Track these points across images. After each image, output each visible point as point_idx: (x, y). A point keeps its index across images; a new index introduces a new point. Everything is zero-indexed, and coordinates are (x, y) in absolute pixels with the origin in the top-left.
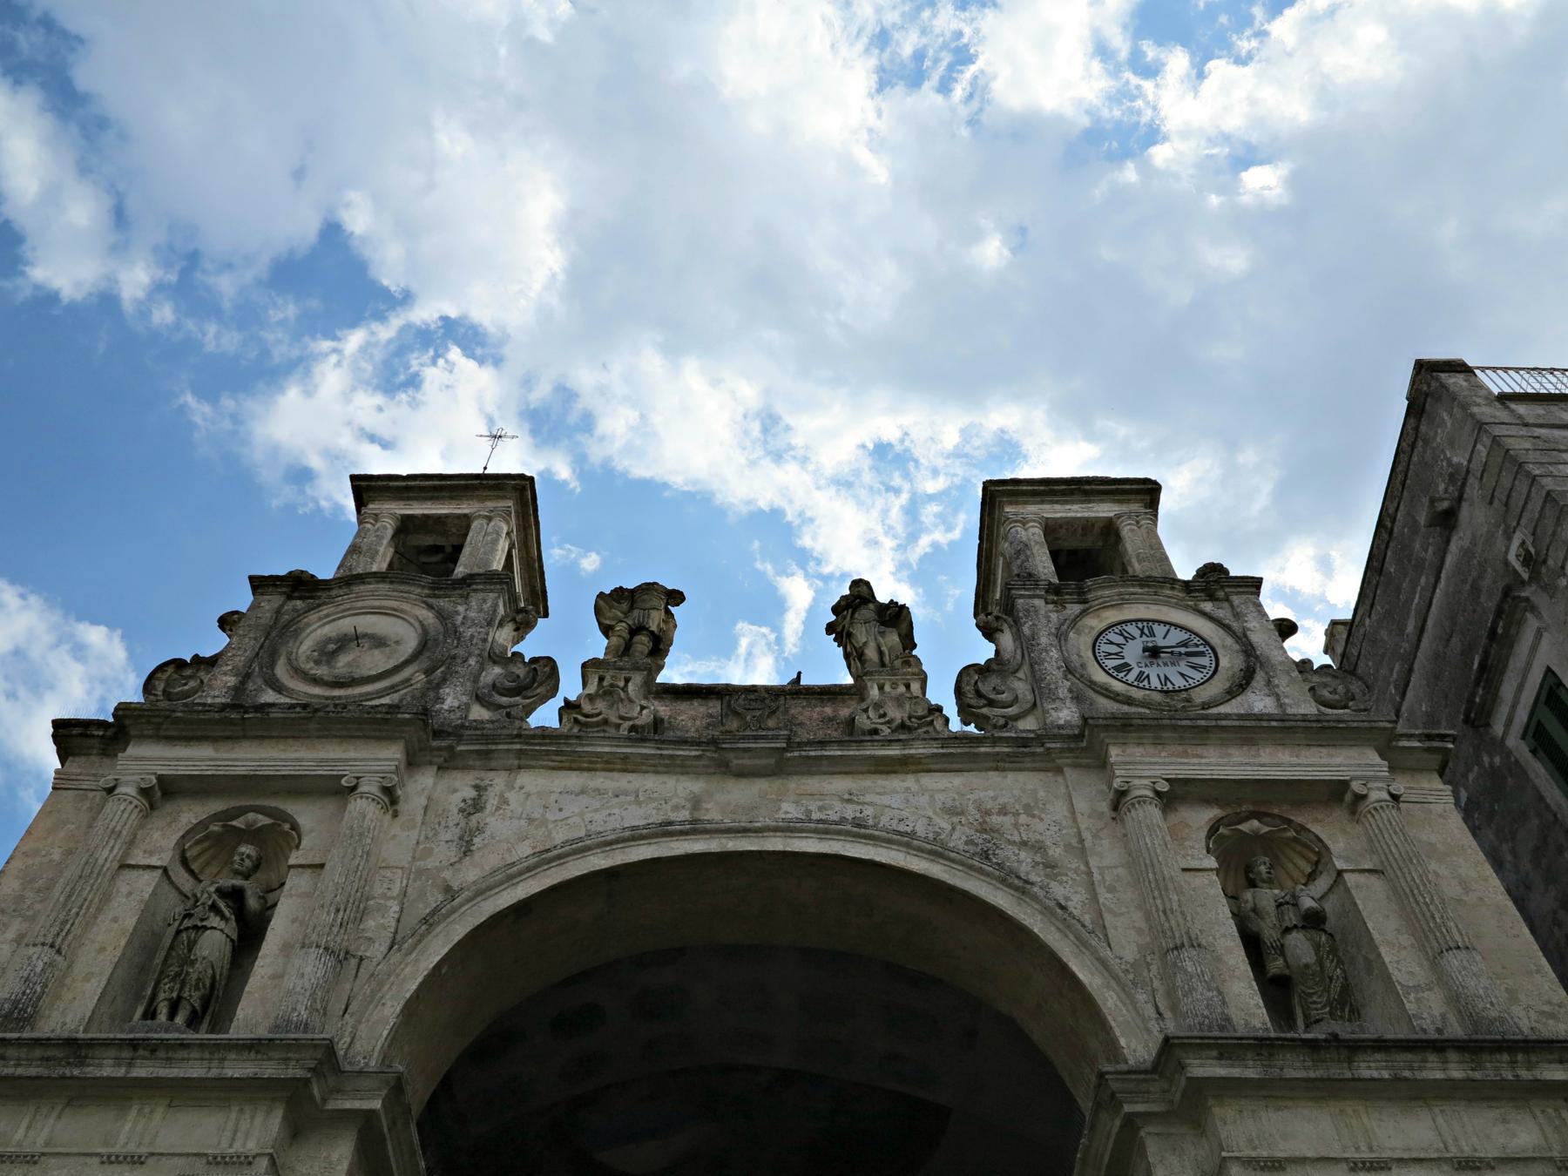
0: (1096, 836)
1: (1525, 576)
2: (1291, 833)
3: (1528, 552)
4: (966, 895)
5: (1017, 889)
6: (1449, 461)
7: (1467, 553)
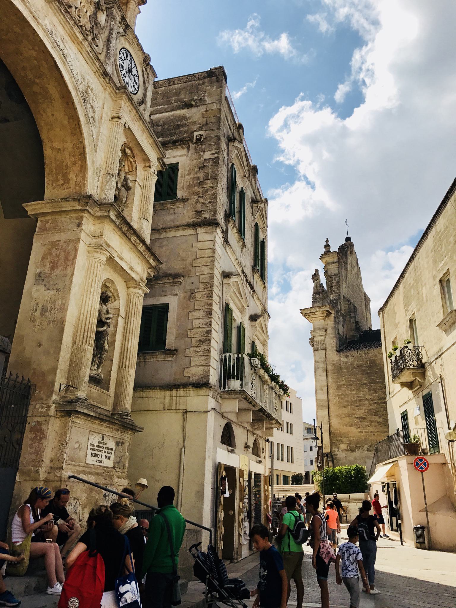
0: (105, 121)
1: (194, 141)
2: (131, 160)
3: (201, 138)
4: (75, 109)
5: (87, 121)
6: (204, 96)
7: (184, 118)
